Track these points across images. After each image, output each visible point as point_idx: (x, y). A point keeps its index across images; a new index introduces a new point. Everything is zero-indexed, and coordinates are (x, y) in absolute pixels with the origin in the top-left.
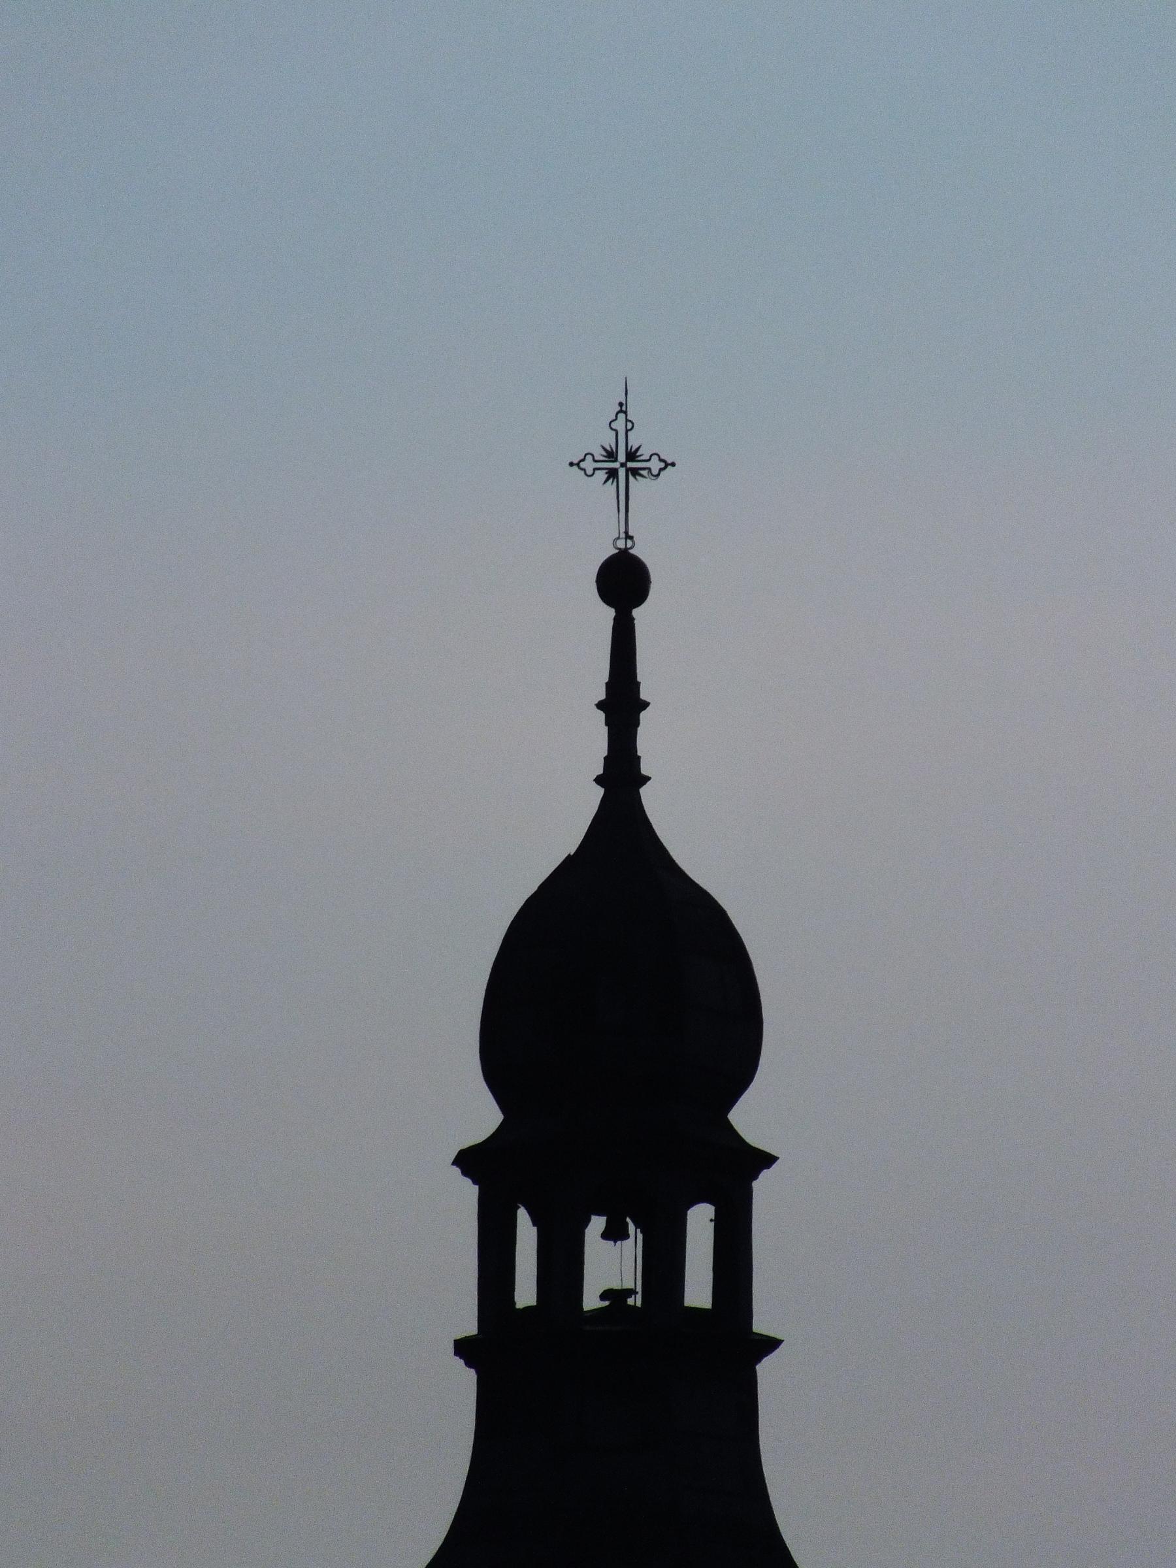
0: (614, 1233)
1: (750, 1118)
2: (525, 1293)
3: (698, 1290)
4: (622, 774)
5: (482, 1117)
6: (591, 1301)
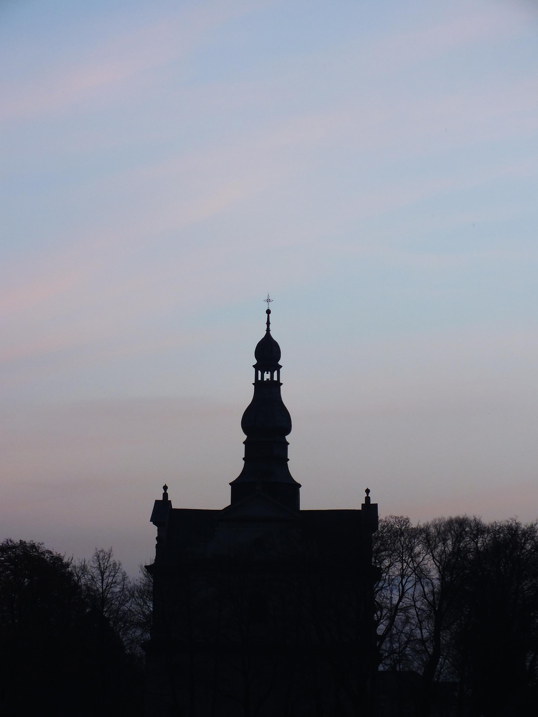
0: (268, 373)
1: (280, 363)
2: (260, 379)
3: (275, 378)
4: (268, 330)
6: (265, 380)
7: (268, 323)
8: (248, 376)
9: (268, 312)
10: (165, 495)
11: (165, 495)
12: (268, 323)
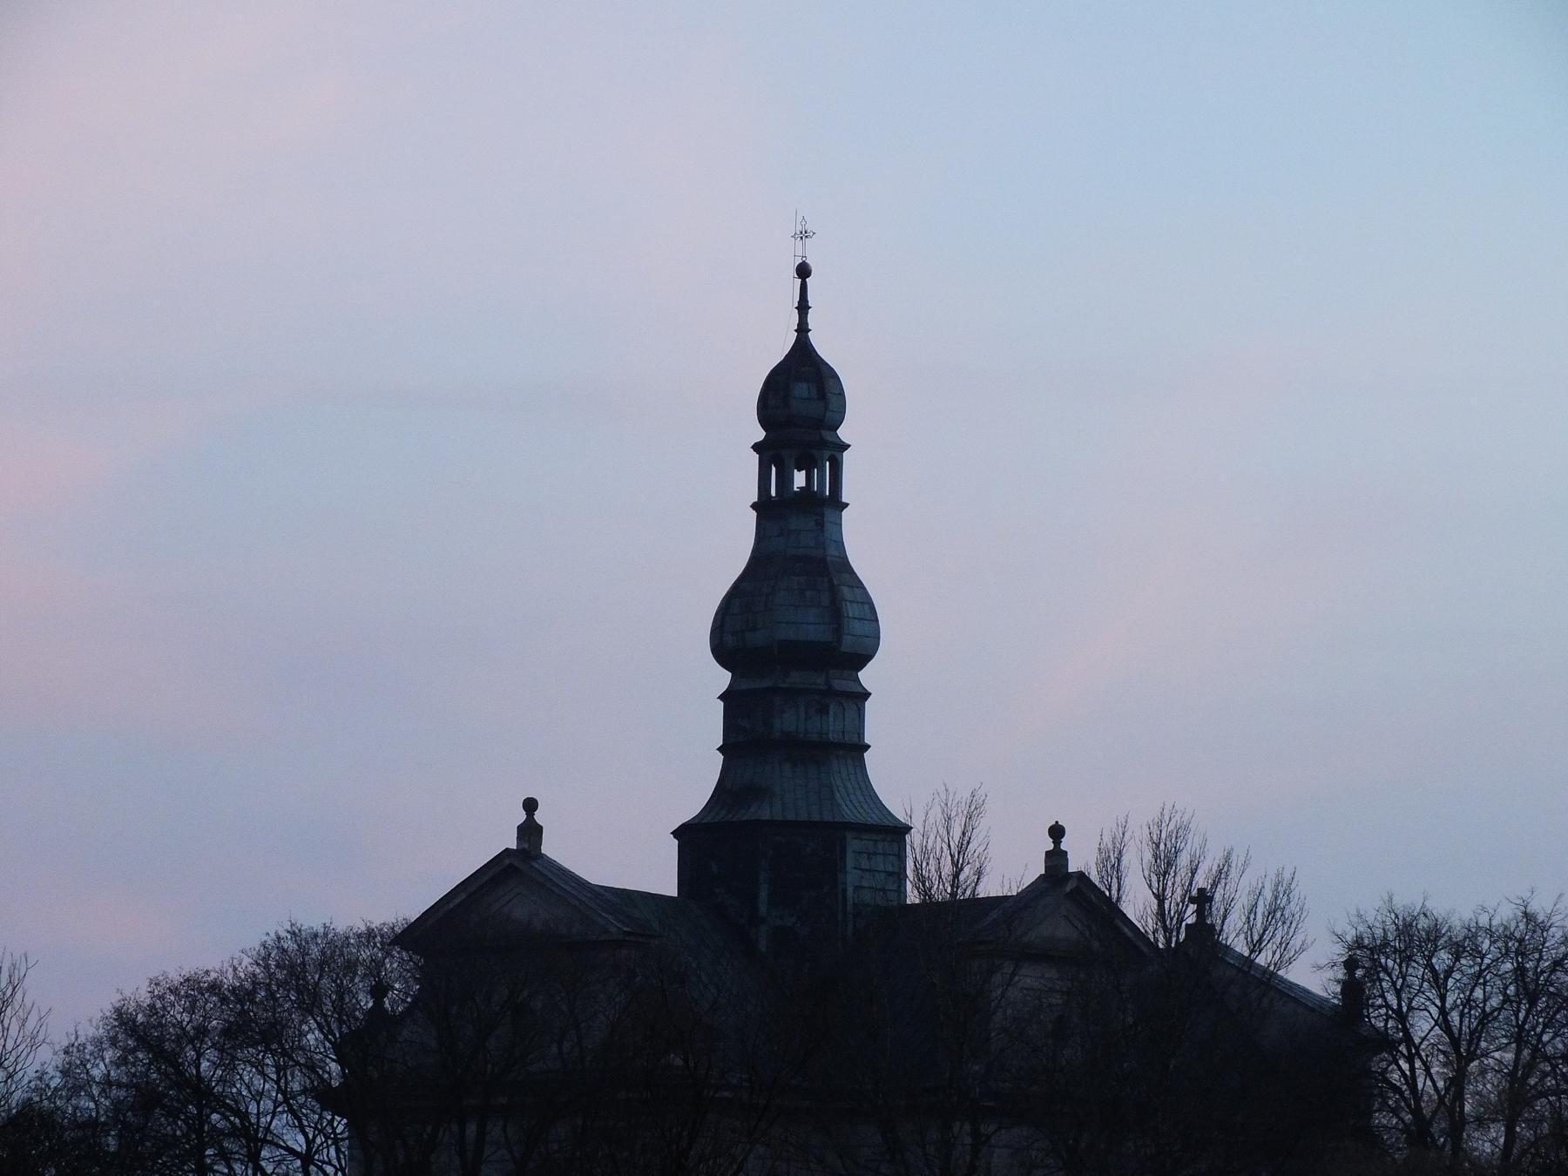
4: (803, 329)
5: (760, 434)
7: (803, 307)
8: (740, 478)
9: (803, 271)
10: (530, 832)
11: (530, 832)
12: (803, 307)
